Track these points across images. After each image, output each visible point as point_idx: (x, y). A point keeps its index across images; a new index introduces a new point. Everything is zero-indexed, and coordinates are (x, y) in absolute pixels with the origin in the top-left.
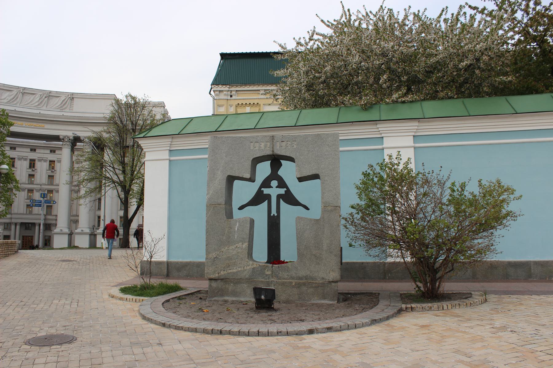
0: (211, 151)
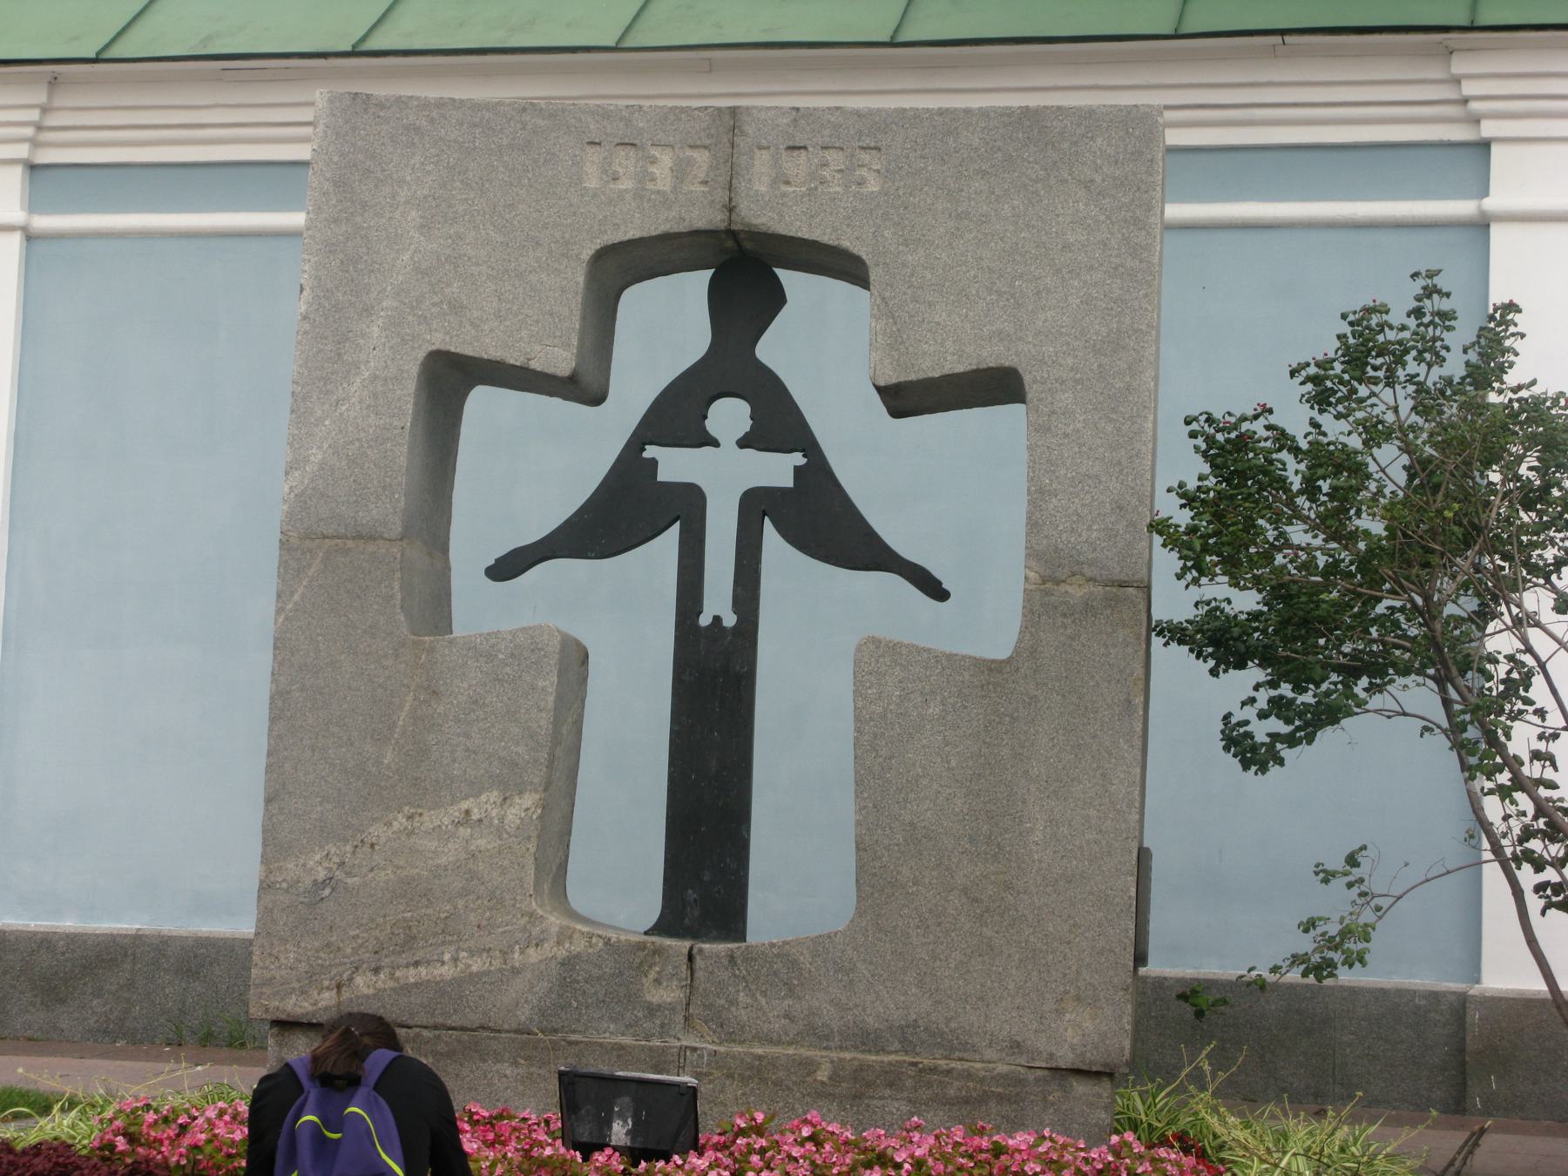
0: (326, 185)
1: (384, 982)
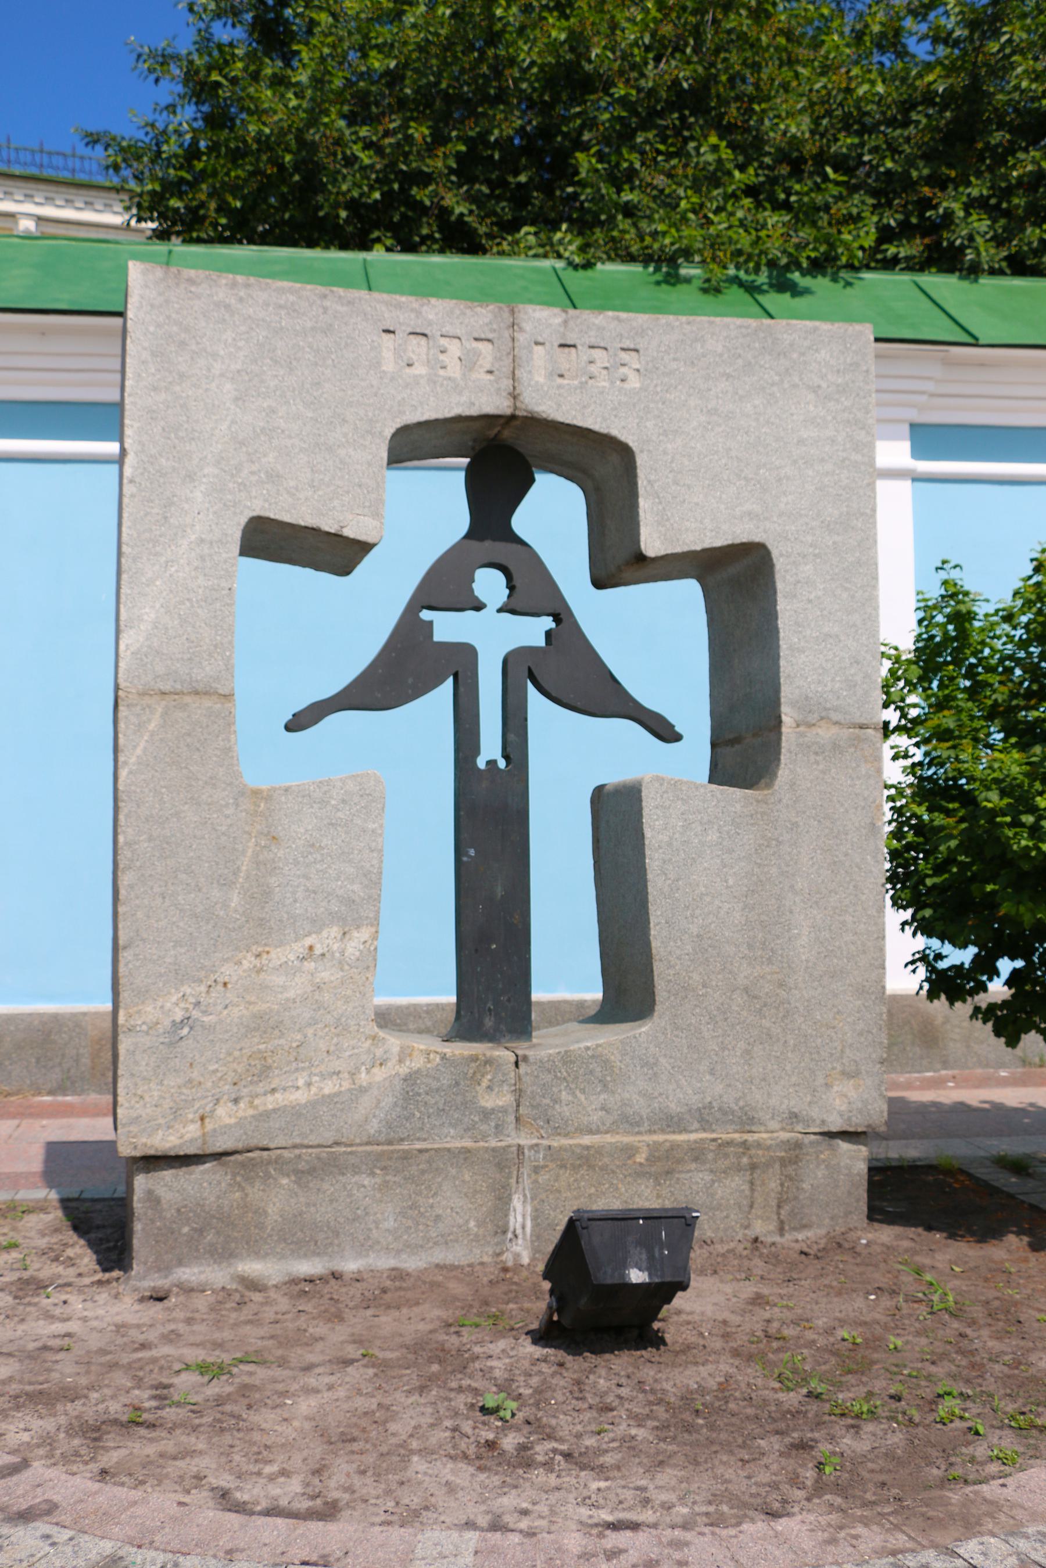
1: (245, 1110)
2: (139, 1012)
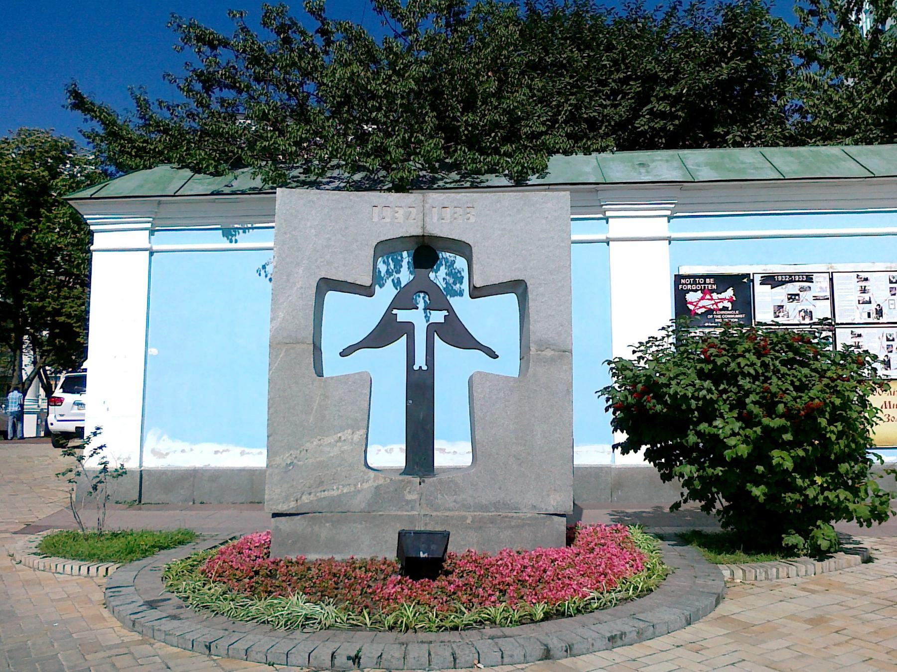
2: (274, 460)
